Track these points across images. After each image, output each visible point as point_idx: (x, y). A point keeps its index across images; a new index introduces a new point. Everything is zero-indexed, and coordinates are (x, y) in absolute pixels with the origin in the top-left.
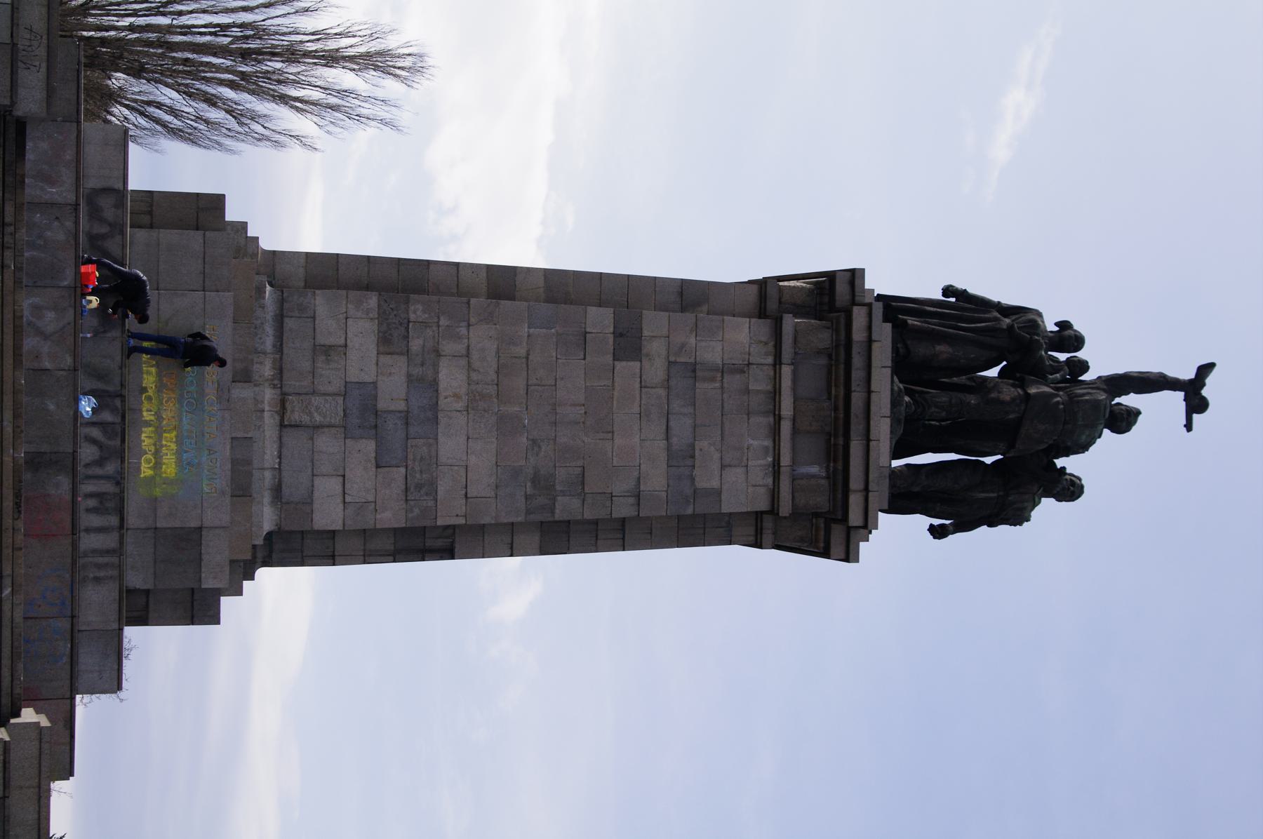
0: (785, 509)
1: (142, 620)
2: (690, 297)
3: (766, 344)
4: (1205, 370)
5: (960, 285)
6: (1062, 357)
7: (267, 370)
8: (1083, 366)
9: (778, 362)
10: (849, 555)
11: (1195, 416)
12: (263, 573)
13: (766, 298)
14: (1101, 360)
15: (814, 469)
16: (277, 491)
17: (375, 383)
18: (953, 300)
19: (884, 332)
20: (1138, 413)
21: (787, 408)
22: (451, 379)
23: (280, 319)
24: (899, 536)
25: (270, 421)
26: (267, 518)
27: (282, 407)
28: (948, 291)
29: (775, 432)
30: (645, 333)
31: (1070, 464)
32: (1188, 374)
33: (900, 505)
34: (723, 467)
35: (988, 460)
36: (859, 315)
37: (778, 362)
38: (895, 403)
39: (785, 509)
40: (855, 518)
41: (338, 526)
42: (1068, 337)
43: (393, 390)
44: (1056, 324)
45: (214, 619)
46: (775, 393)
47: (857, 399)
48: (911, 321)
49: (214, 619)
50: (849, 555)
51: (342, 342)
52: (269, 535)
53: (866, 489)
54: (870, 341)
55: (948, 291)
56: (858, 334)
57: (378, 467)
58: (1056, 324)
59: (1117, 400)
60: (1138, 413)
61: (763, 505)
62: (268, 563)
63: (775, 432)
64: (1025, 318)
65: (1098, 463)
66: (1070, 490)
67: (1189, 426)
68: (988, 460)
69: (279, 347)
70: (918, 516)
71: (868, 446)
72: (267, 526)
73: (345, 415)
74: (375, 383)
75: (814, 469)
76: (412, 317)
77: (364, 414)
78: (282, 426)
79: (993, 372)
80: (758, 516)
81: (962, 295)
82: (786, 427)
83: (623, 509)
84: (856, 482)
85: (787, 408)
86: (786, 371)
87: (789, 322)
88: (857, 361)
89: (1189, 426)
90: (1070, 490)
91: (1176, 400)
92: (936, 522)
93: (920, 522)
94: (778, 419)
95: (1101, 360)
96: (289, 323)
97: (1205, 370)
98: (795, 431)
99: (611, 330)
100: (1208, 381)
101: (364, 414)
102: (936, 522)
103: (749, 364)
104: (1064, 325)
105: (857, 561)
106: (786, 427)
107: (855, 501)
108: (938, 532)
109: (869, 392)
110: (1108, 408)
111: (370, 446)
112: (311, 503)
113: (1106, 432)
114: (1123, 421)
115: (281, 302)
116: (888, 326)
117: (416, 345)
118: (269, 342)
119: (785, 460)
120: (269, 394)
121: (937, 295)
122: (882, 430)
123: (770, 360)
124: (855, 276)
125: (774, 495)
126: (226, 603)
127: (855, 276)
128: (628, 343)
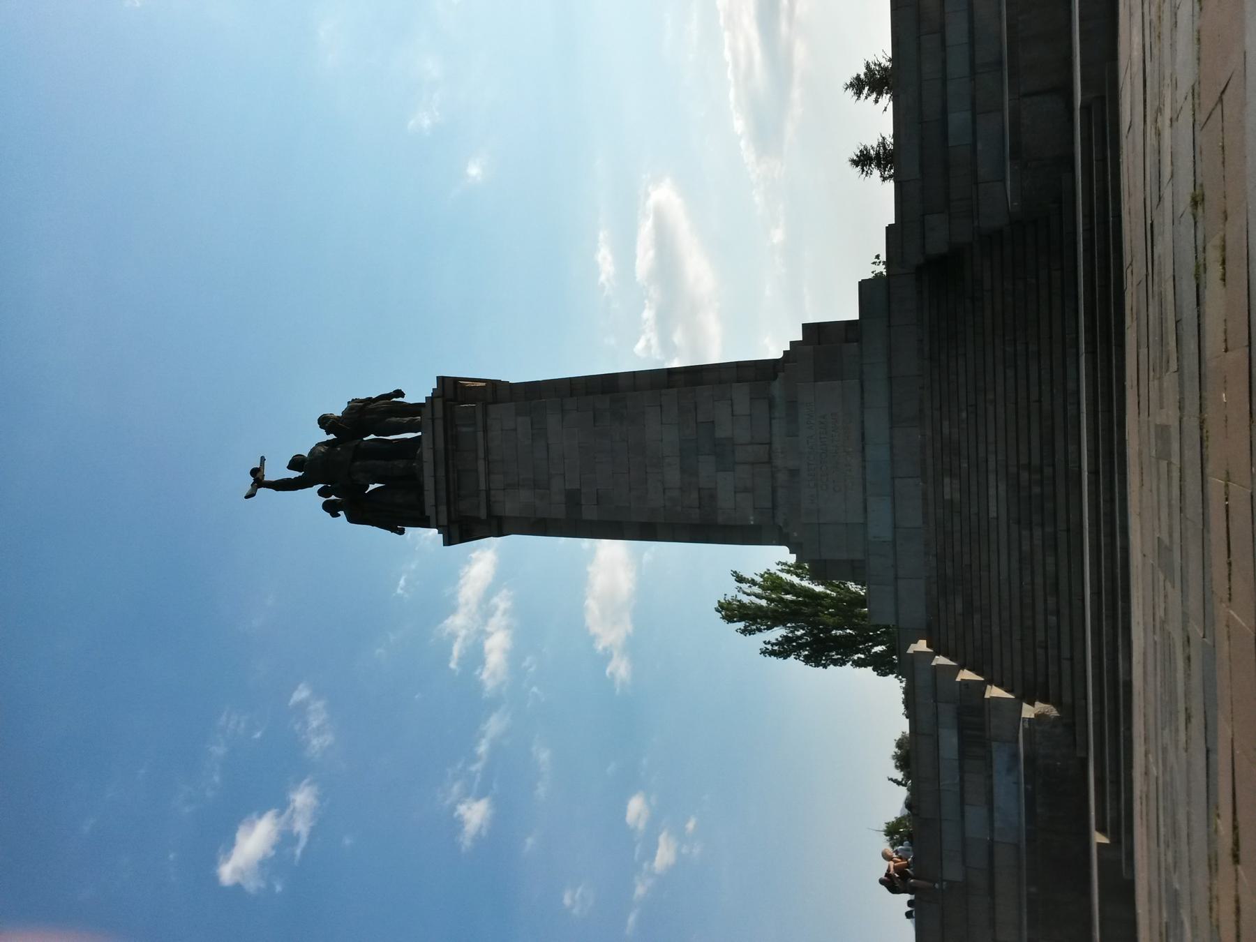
1: (849, 324)
6: (333, 497)
7: (782, 477)
8: (321, 493)
9: (488, 491)
10: (442, 380)
12: (779, 355)
13: (498, 527)
14: (311, 497)
15: (464, 429)
16: (771, 406)
19: (430, 511)
20: (290, 467)
22: (673, 476)
23: (774, 507)
24: (418, 392)
26: (777, 388)
28: (401, 532)
29: (487, 451)
33: (416, 409)
34: (515, 430)
35: (372, 436)
36: (443, 520)
37: (488, 491)
38: (422, 470)
40: (439, 404)
42: (331, 508)
45: (806, 327)
46: (488, 473)
47: (441, 472)
49: (806, 327)
50: (442, 380)
52: (775, 377)
54: (436, 506)
55: (401, 532)
56: (443, 508)
60: (290, 467)
61: (492, 408)
62: (774, 362)
63: (487, 451)
67: (263, 459)
68: (372, 436)
69: (774, 491)
78: (770, 444)
79: (372, 487)
80: (495, 402)
81: (394, 530)
82: (481, 454)
86: (483, 486)
87: (483, 514)
88: (443, 494)
89: (263, 459)
91: (270, 476)
92: (400, 399)
94: (486, 458)
95: (311, 497)
102: (400, 399)
104: (335, 515)
107: (439, 413)
108: (399, 393)
109: (435, 476)
110: (308, 470)
111: (721, 433)
114: (296, 463)
115: (773, 517)
119: (480, 434)
121: (407, 529)
122: (427, 455)
123: (493, 492)
124: (448, 541)
125: (486, 414)
126: (799, 337)
127: (448, 541)
128: (573, 499)
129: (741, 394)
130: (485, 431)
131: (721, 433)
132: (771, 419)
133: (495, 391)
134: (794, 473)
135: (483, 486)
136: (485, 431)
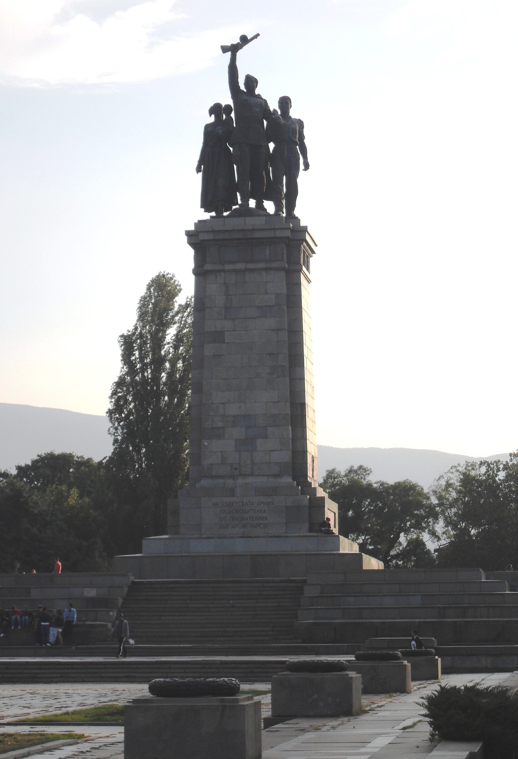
3: (216, 276)
4: (225, 49)
5: (196, 164)
7: (230, 482)
9: (223, 271)
11: (249, 38)
15: (268, 251)
16: (276, 476)
17: (236, 440)
18: (202, 166)
21: (241, 266)
22: (233, 410)
25: (250, 480)
26: (288, 480)
27: (245, 475)
30: (213, 330)
31: (274, 105)
32: (229, 54)
34: (266, 293)
36: (202, 237)
37: (223, 271)
41: (290, 453)
43: (238, 433)
44: (210, 116)
46: (236, 271)
47: (236, 236)
51: (220, 454)
53: (274, 229)
55: (198, 170)
56: (211, 237)
57: (267, 438)
58: (210, 116)
59: (242, 87)
61: (283, 274)
64: (210, 132)
65: (270, 94)
66: (285, 103)
67: (257, 35)
69: (222, 477)
70: (299, 180)
71: (256, 229)
72: (290, 480)
73: (247, 451)
74: (236, 440)
75: (268, 251)
76: (210, 426)
77: (246, 444)
78: (252, 475)
81: (201, 162)
82: (251, 266)
84: (271, 234)
85: (241, 266)
86: (227, 267)
87: (208, 267)
88: (221, 236)
89: (257, 35)
90: (285, 103)
94: (246, 270)
96: (214, 474)
97: (225, 49)
98: (252, 261)
99: (212, 344)
100: (229, 45)
101: (246, 444)
102: (302, 167)
103: (225, 283)
105: (306, 227)
106: (251, 266)
107: (279, 234)
108: (307, 166)
109: (234, 230)
111: (259, 442)
112: (280, 463)
113: (257, 92)
114: (251, 82)
116: (209, 218)
117: (220, 425)
118: (221, 481)
119: (262, 265)
120: (240, 481)
121: (201, 174)
123: (223, 274)
124: (189, 234)
127: (189, 234)
128: (218, 337)
129: (285, 456)
130: (266, 269)
131: (259, 442)
132: (268, 476)
134: (232, 492)
135: (227, 267)
136: (266, 269)
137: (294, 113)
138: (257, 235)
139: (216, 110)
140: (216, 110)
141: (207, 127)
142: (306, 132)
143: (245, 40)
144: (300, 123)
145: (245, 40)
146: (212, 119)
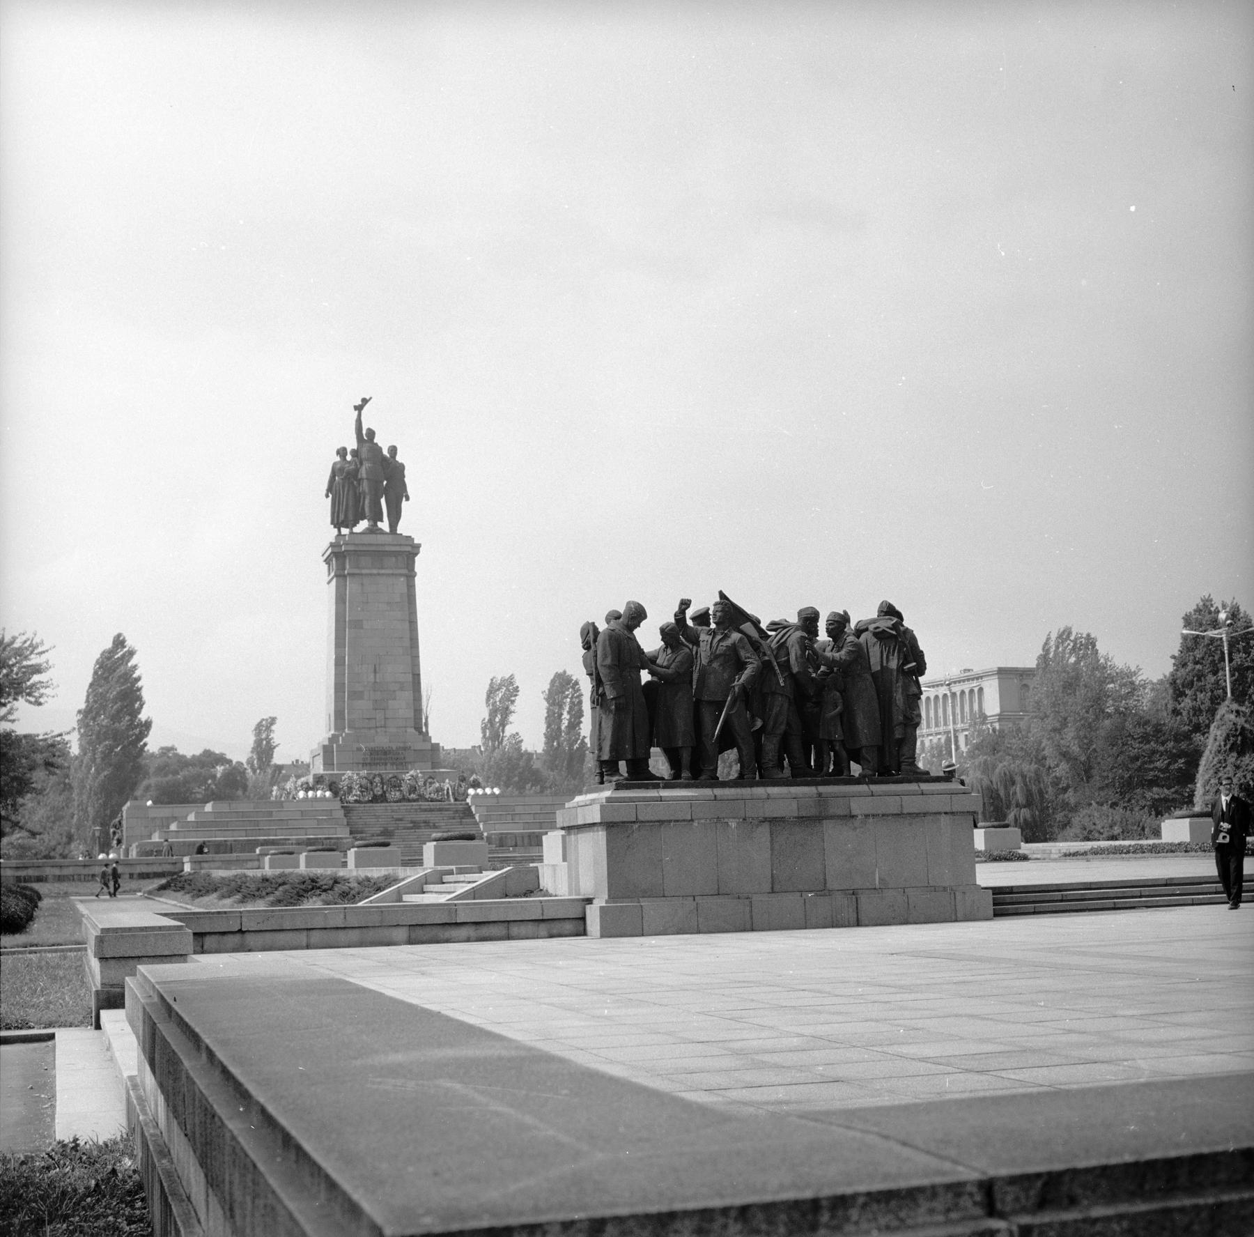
0: (405, 571)
2: (340, 599)
6: (349, 458)
10: (419, 546)
13: (340, 576)
21: (375, 571)
31: (385, 452)
39: (405, 571)
40: (409, 549)
48: (342, 517)
55: (327, 496)
66: (393, 450)
81: (330, 490)
82: (383, 571)
83: (407, 625)
84: (398, 549)
85: (375, 571)
86: (364, 571)
88: (361, 548)
93: (404, 504)
95: (352, 444)
108: (408, 499)
110: (366, 438)
114: (371, 433)
125: (401, 575)
128: (357, 624)
133: (411, 576)
137: (399, 458)
138: (387, 549)
139: (342, 452)
140: (342, 452)
141: (335, 464)
142: (406, 472)
143: (365, 401)
144: (402, 467)
145: (365, 401)
146: (338, 459)
